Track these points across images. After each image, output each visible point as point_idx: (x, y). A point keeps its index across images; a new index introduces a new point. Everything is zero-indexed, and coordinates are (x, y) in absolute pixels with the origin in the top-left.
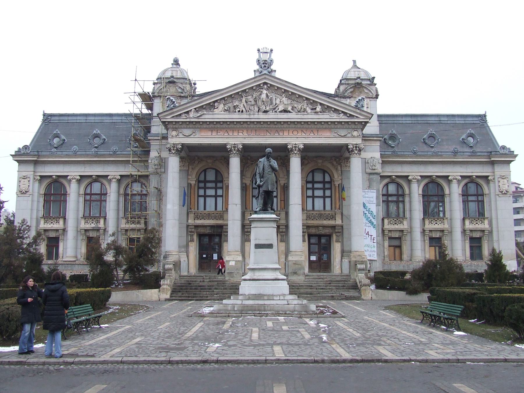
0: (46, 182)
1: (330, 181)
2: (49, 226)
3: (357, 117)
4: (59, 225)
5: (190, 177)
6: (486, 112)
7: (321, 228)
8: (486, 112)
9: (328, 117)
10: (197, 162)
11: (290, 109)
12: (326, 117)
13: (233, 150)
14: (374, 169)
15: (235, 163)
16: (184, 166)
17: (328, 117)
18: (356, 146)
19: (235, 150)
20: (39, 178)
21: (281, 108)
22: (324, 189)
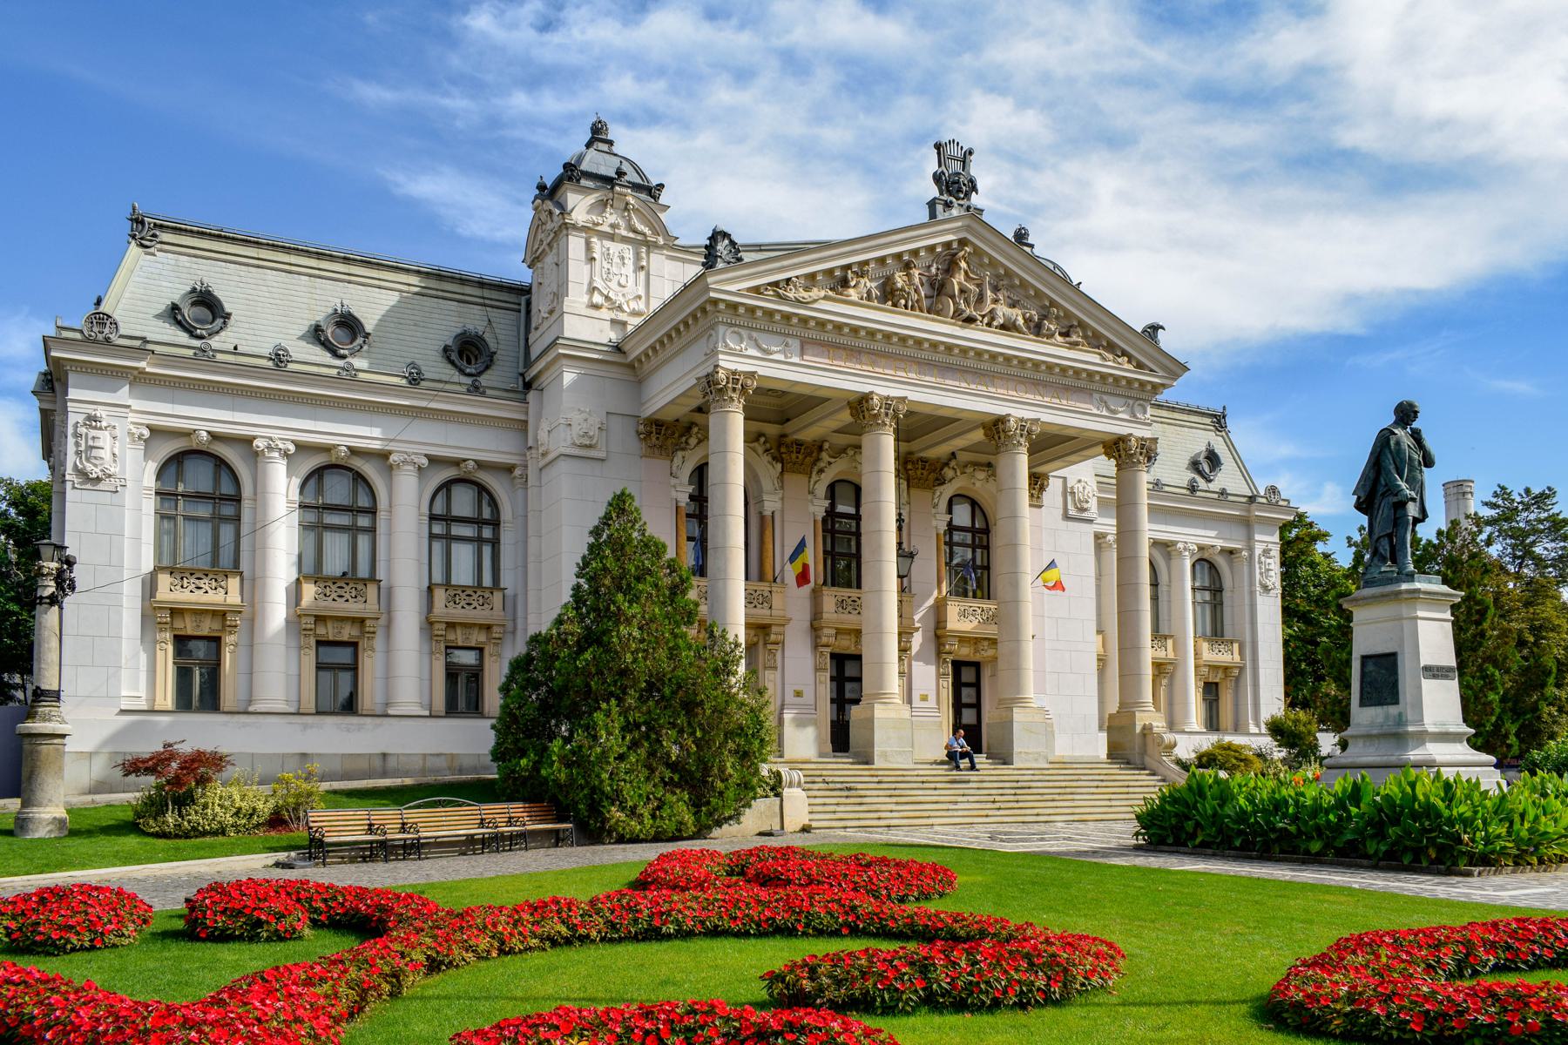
0: (168, 448)
1: (984, 527)
2: (185, 596)
3: (1151, 370)
4: (230, 594)
5: (673, 481)
6: (1224, 408)
7: (986, 643)
8: (1224, 408)
10: (693, 441)
12: (1088, 359)
13: (883, 415)
14: (1086, 510)
15: (886, 445)
16: (661, 447)
17: (1096, 359)
19: (887, 414)
20: (146, 433)
22: (974, 547)
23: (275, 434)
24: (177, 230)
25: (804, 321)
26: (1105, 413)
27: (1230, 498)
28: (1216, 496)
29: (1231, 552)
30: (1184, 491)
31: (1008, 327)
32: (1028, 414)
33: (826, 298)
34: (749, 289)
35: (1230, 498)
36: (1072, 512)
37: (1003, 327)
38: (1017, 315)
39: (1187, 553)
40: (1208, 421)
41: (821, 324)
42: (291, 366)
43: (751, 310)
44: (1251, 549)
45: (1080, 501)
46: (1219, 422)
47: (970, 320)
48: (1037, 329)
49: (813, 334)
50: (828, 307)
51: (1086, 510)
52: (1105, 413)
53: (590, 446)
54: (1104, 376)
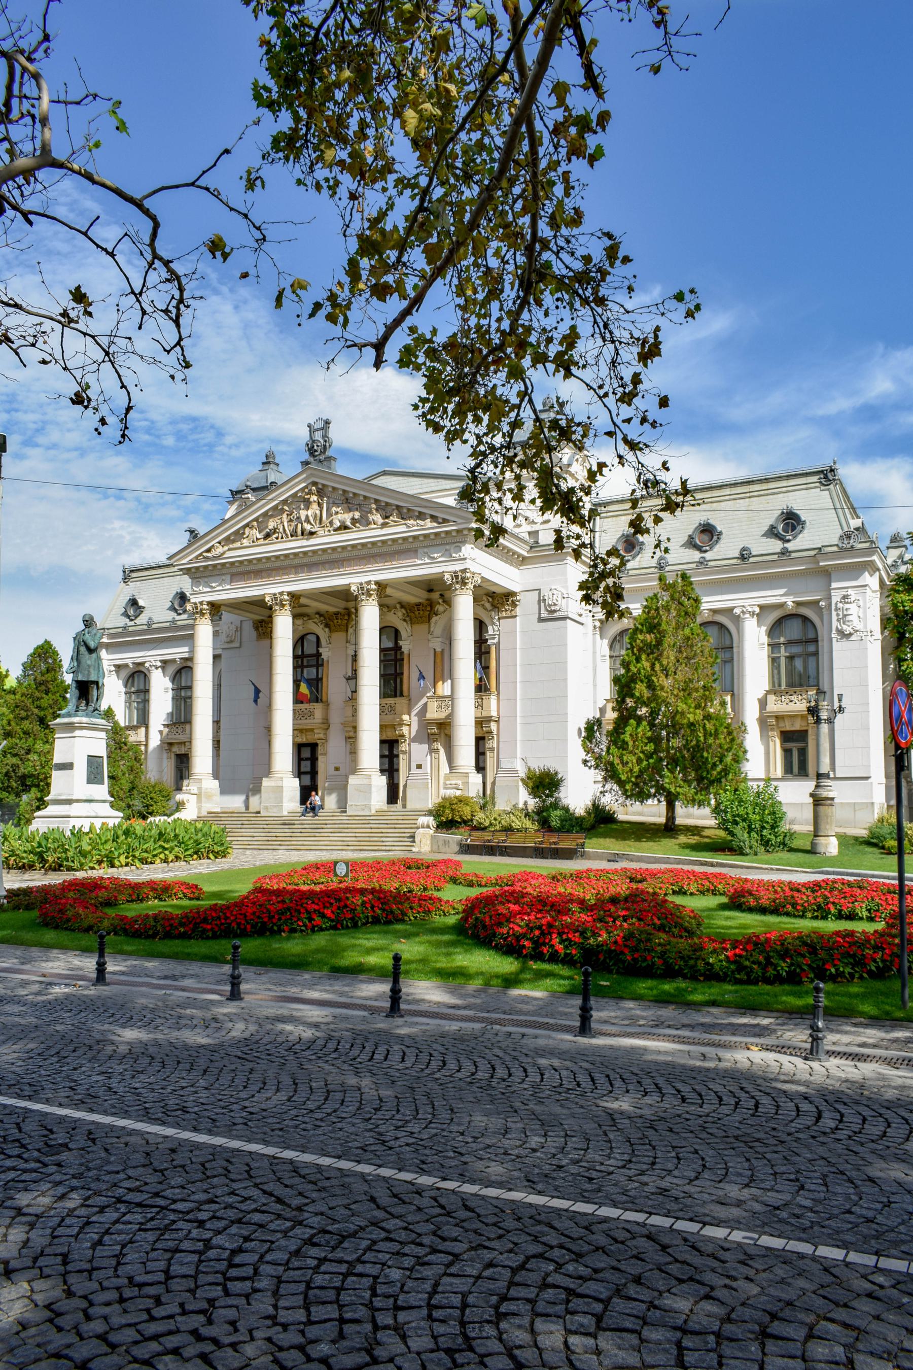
9: (403, 528)
11: (348, 523)
14: (555, 611)
17: (403, 528)
18: (455, 575)
21: (337, 524)
23: (152, 659)
24: (138, 570)
25: (223, 565)
26: (427, 561)
27: (794, 555)
28: (775, 557)
29: (817, 602)
30: (734, 561)
31: (344, 527)
32: (364, 579)
33: (229, 550)
34: (196, 558)
35: (794, 555)
36: (544, 614)
37: (339, 529)
38: (347, 517)
39: (747, 616)
40: (815, 479)
41: (232, 563)
42: (154, 626)
43: (197, 568)
44: (829, 598)
45: (550, 606)
46: (826, 477)
47: (312, 533)
48: (364, 521)
49: (234, 570)
50: (234, 554)
51: (555, 611)
52: (427, 561)
53: (231, 642)
54: (415, 537)
